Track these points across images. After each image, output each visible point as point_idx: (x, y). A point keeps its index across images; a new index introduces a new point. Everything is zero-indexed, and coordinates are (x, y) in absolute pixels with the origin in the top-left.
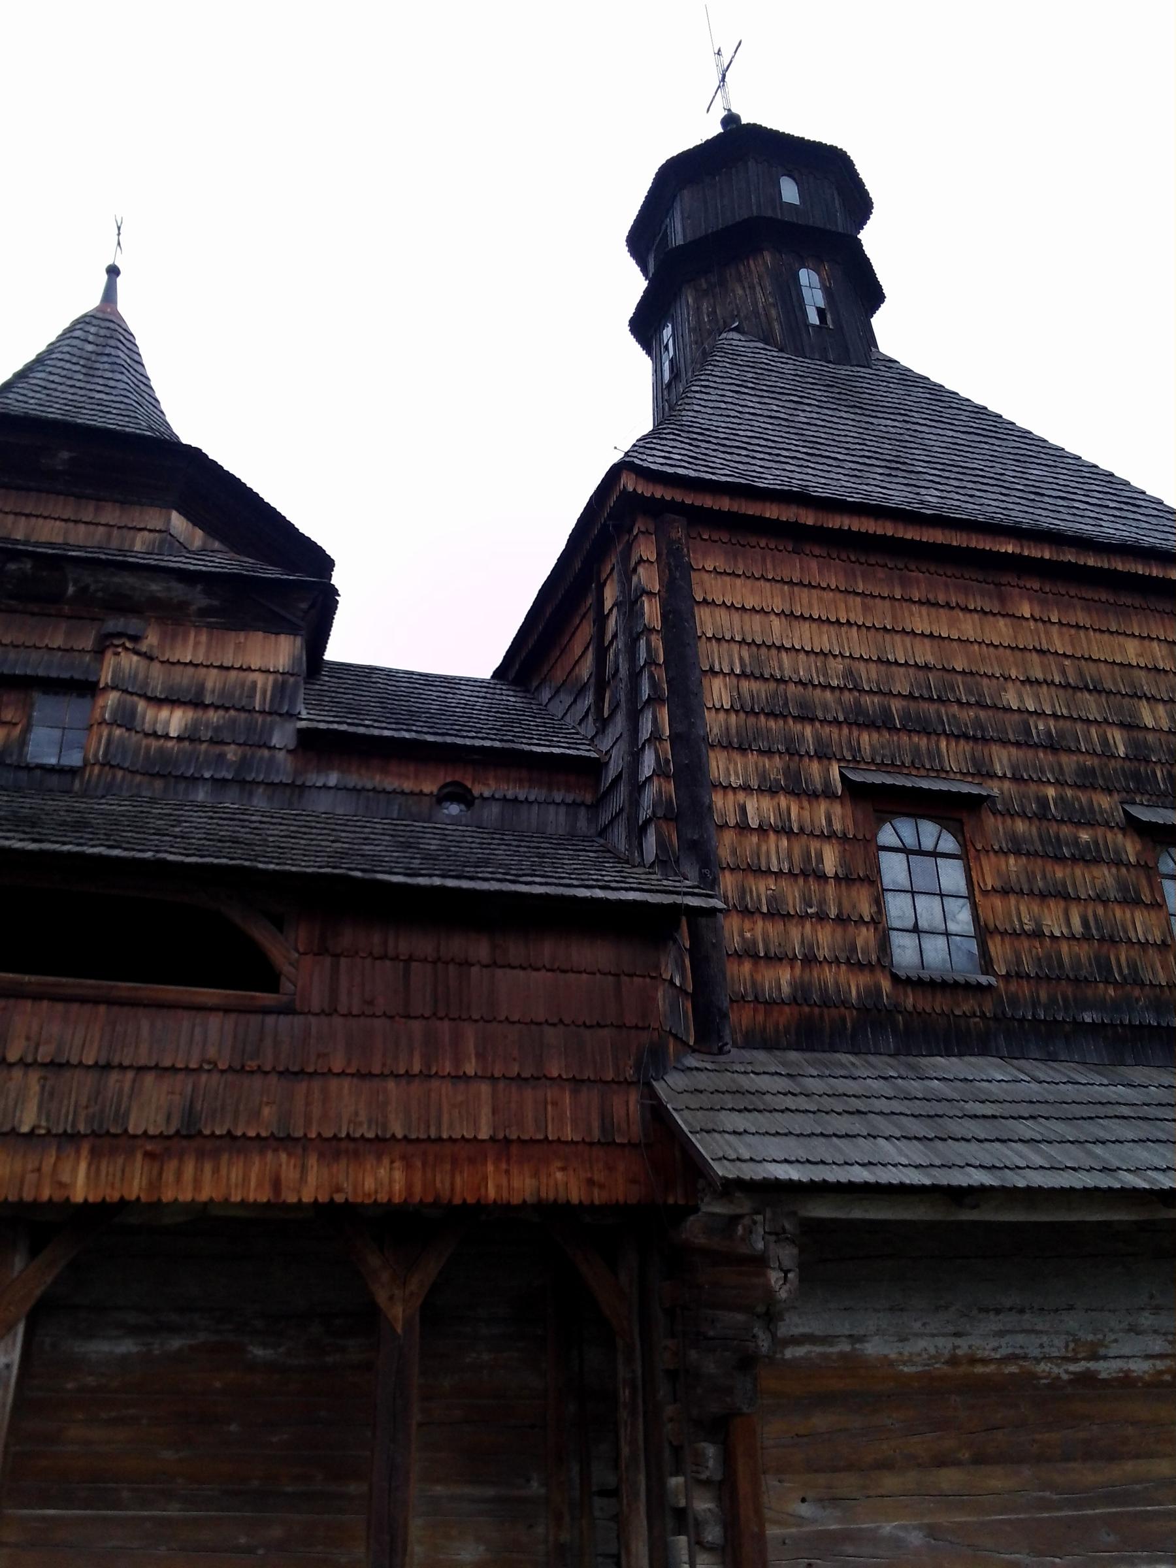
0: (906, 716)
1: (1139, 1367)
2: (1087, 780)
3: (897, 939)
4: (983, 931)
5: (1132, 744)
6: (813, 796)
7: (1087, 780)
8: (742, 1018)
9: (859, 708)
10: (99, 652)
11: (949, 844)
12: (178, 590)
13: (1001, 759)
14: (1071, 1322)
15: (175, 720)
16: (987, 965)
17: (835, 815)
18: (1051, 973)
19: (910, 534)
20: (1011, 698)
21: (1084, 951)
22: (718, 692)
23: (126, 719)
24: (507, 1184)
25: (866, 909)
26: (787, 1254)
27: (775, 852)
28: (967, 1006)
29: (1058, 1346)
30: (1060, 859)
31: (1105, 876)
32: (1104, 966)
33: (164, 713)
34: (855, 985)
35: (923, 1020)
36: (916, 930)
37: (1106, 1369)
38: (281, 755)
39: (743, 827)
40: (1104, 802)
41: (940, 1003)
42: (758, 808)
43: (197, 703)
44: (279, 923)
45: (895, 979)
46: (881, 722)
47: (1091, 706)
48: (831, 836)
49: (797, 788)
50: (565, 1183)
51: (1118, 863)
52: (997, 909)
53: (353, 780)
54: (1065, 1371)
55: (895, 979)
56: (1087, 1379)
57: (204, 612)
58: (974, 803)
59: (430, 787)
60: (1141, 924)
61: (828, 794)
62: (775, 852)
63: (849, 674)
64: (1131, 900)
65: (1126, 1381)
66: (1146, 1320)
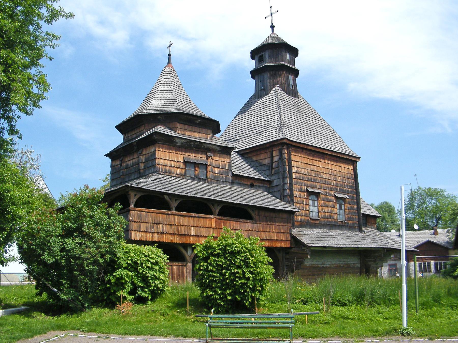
0: (314, 179)
1: (328, 265)
2: (331, 189)
3: (311, 213)
4: (319, 212)
5: (336, 184)
6: (303, 192)
7: (331, 189)
8: (296, 223)
9: (308, 178)
10: (207, 159)
11: (316, 199)
12: (216, 147)
13: (323, 186)
14: (322, 260)
15: (217, 170)
16: (319, 217)
17: (305, 194)
18: (325, 217)
19: (316, 150)
20: (325, 176)
21: (328, 214)
22: (294, 174)
23: (212, 171)
24: (278, 245)
25: (308, 209)
26: (310, 253)
27: (299, 200)
28: (317, 222)
29: (321, 263)
30: (327, 201)
31: (331, 203)
32: (330, 216)
33: (215, 169)
34: (306, 219)
35: (312, 224)
36: (312, 211)
37: (325, 266)
38: (230, 177)
39: (296, 197)
40: (332, 192)
41: (313, 222)
42: (297, 193)
43: (219, 168)
44: (253, 210)
45: (310, 218)
46: (310, 181)
47: (332, 177)
48: (305, 198)
49: (301, 191)
50: (283, 245)
51: (333, 202)
52: (320, 209)
53: (239, 182)
54: (321, 266)
55: (310, 218)
56: (323, 267)
57: (218, 151)
58: (319, 193)
59: (249, 184)
60: (334, 210)
61: (305, 192)
62: (299, 200)
63: (308, 172)
64: (334, 207)
65: (326, 267)
66: (329, 260)
